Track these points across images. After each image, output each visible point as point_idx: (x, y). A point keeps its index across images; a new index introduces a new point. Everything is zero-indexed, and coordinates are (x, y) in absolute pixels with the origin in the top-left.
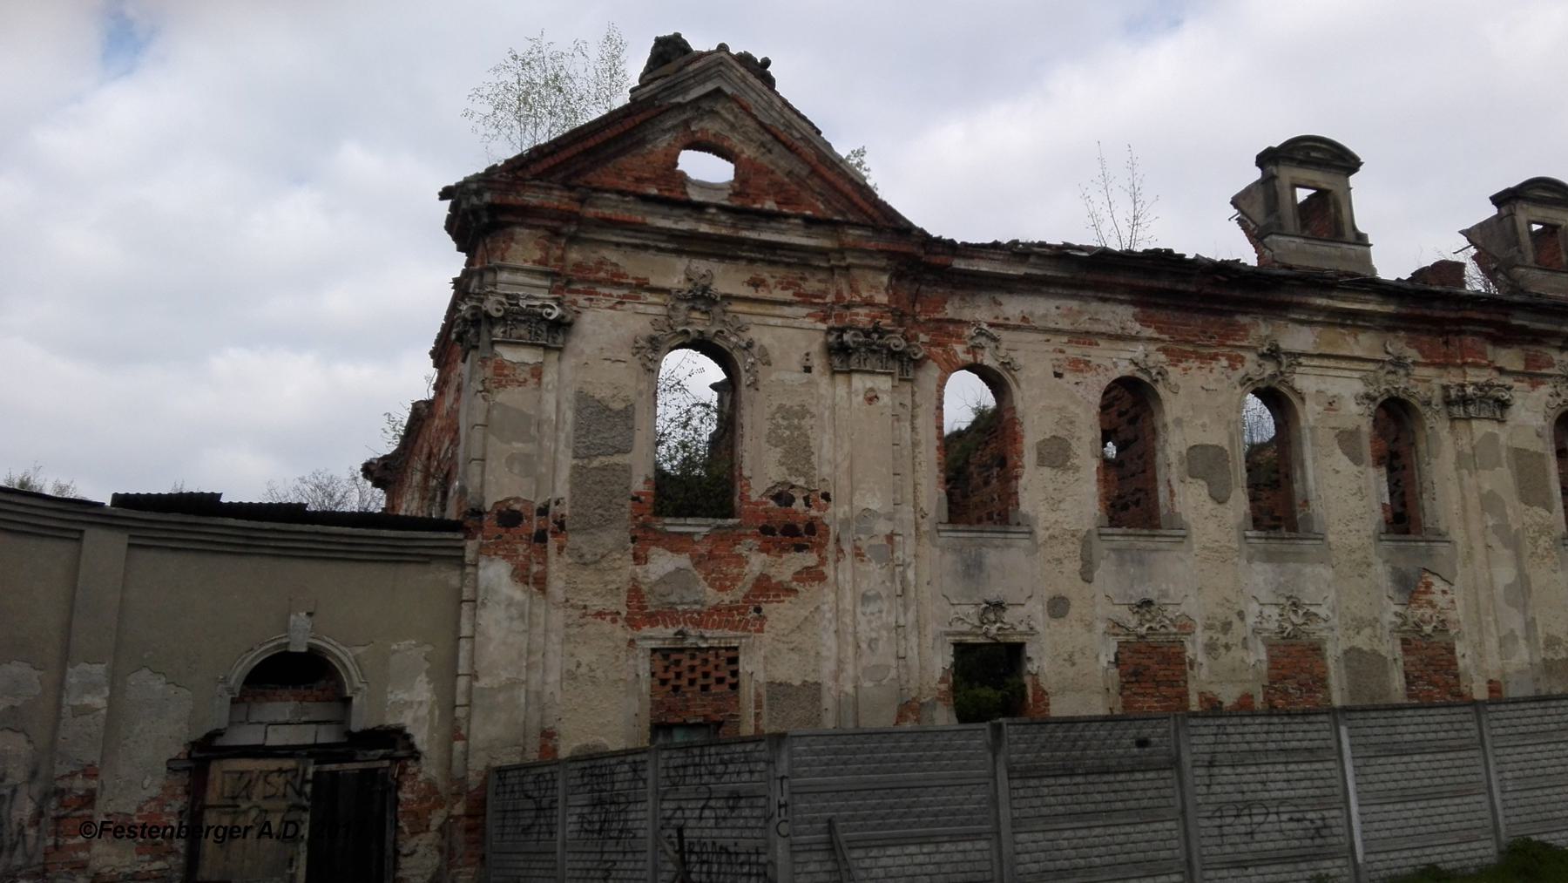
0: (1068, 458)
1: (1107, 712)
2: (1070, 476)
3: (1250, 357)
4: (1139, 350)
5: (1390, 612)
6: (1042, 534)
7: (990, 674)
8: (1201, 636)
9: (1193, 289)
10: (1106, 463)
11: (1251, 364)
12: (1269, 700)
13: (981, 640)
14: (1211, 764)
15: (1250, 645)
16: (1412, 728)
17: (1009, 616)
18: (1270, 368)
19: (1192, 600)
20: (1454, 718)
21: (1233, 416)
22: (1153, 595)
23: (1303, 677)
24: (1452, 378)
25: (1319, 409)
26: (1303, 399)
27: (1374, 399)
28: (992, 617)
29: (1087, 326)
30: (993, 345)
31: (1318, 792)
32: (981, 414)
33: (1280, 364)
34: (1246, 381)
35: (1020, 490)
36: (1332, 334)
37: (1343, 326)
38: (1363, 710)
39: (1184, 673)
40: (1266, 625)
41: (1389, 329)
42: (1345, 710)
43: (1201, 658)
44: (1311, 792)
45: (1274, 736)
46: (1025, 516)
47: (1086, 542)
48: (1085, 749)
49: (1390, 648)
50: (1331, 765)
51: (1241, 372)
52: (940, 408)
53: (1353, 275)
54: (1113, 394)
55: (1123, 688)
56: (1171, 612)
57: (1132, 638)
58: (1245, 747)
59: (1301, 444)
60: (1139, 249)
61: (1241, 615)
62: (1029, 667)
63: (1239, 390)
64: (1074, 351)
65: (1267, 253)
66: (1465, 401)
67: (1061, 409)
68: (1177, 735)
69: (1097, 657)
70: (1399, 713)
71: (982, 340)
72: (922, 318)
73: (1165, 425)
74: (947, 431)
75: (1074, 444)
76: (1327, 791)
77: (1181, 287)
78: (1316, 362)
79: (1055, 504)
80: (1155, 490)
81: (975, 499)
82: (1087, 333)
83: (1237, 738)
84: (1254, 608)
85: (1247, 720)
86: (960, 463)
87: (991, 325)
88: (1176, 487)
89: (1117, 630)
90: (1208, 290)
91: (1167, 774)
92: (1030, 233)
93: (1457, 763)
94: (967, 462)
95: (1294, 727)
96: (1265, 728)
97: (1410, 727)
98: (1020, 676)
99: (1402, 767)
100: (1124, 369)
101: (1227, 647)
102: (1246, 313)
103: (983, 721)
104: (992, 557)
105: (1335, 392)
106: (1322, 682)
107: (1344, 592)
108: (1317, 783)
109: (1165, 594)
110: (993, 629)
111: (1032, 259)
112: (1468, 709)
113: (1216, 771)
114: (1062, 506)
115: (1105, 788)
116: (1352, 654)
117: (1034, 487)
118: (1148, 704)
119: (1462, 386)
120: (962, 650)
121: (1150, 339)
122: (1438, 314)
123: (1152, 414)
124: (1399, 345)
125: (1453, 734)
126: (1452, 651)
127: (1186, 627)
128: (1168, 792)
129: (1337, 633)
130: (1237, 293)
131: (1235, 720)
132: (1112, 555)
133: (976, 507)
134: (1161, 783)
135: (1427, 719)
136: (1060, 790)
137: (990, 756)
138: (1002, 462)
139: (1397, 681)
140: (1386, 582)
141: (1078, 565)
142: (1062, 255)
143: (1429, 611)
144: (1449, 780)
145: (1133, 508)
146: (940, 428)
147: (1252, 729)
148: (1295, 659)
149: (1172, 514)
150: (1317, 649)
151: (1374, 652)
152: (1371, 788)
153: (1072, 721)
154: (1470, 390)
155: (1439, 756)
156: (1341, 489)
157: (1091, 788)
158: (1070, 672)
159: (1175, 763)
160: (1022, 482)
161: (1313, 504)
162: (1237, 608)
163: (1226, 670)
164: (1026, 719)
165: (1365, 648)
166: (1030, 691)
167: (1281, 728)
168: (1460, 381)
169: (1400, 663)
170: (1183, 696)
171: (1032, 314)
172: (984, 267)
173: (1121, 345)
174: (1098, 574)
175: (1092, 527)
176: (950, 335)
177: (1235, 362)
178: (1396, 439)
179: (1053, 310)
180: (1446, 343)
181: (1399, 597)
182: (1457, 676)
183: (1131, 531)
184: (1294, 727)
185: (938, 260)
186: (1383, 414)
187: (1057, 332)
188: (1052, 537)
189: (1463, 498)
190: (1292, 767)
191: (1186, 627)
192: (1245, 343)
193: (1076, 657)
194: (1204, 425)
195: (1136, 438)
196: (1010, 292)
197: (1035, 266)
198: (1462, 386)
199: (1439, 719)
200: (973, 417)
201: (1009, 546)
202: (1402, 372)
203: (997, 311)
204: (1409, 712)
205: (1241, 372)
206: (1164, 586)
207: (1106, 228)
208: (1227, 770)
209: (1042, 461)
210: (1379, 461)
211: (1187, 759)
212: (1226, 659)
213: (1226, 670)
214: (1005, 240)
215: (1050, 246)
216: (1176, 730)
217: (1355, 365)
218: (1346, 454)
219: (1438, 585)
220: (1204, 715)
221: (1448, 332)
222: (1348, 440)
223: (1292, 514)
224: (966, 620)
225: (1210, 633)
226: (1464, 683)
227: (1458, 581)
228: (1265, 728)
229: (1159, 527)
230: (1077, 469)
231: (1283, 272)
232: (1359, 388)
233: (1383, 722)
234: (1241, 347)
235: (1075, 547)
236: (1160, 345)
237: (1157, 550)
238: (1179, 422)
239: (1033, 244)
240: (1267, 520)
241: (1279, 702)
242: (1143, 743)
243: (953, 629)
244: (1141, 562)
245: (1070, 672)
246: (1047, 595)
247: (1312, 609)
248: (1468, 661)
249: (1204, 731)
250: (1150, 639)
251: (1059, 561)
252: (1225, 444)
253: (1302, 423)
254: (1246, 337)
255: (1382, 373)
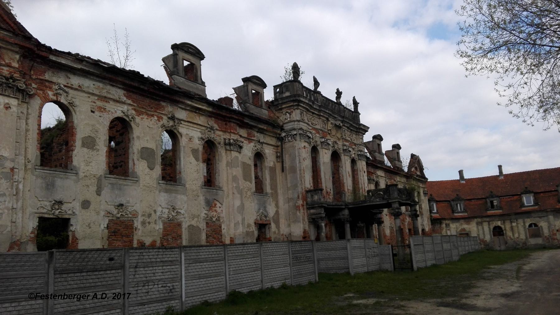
0: (95, 145)
1: (101, 247)
2: (95, 153)
3: (165, 118)
4: (125, 108)
6: (81, 175)
7: (54, 231)
8: (140, 219)
9: (146, 88)
10: (111, 150)
11: (165, 120)
12: (162, 243)
13: (51, 216)
14: (136, 267)
15: (157, 222)
16: (205, 253)
17: (64, 207)
18: (171, 123)
19: (138, 205)
20: (217, 250)
21: (158, 138)
22: (124, 202)
23: (174, 235)
24: (227, 136)
25: (187, 140)
26: (181, 136)
27: (204, 140)
28: (57, 207)
29: (105, 95)
30: (65, 94)
31: (172, 276)
32: (60, 122)
33: (175, 122)
34: (163, 126)
35: (73, 156)
36: (192, 115)
37: (196, 112)
38: (190, 247)
39: (133, 232)
40: (163, 216)
41: (210, 117)
42: (185, 247)
43: (140, 227)
44: (170, 276)
45: (160, 256)
46: (75, 167)
47: (99, 179)
48: (88, 262)
49: (203, 225)
50: (177, 266)
51: (161, 123)
52: (40, 117)
53: (199, 95)
54: (115, 123)
55: (109, 238)
56: (130, 209)
57: (114, 218)
58: (149, 260)
59: (180, 152)
60: (127, 69)
61: (155, 211)
62: (71, 228)
63: (160, 129)
64: (99, 103)
65: (173, 81)
66: (230, 144)
67: (93, 125)
68: (125, 255)
69: (100, 225)
70: (201, 248)
71: (61, 92)
72: (34, 77)
73: (133, 138)
74: (43, 127)
75: (97, 140)
76: (175, 276)
77: (142, 87)
78: (186, 124)
79: (88, 163)
80: (128, 162)
81: (55, 157)
82: (105, 97)
83: (147, 257)
84: (160, 209)
85: (151, 250)
86: (49, 141)
87: (65, 86)
88: (136, 162)
89: (108, 215)
90: (152, 90)
91: (119, 271)
92: (85, 52)
93: (217, 265)
94: (52, 141)
95: (167, 253)
96: (157, 253)
97: (204, 253)
98: (67, 232)
99: (200, 267)
100: (119, 114)
101: (149, 223)
102: (164, 102)
103: (46, 251)
104: (59, 182)
105: (192, 135)
106: (180, 237)
107: (189, 206)
108: (172, 273)
109: (128, 202)
110: (57, 212)
111: (84, 63)
112: (222, 247)
113: (137, 269)
114: (91, 164)
115: (94, 277)
116: (191, 227)
117: (79, 155)
118: (118, 244)
119: (230, 139)
120: (42, 220)
121: (130, 104)
122: (224, 114)
123: (129, 133)
124: (212, 122)
125: (216, 256)
126: (221, 227)
127: (135, 215)
128: (119, 278)
129: (186, 219)
130: (161, 94)
131: (147, 250)
132: (110, 186)
133: (55, 161)
134: (117, 275)
135: (210, 250)
136: (76, 278)
137: (47, 265)
138: (67, 143)
139: (204, 237)
141: (95, 188)
142: (97, 64)
143: (215, 213)
144: (214, 271)
145: (119, 168)
146: (39, 125)
147: (153, 253)
148: (172, 228)
149: (134, 172)
150: (179, 225)
151: (198, 227)
152: (189, 274)
153: (84, 251)
154: (232, 141)
155: (212, 263)
156: (191, 169)
157: (89, 277)
158: (88, 231)
159: (123, 267)
160: (75, 153)
161: (183, 174)
162: (154, 209)
163: (147, 232)
164: (65, 250)
165: (195, 225)
166: (70, 238)
167: (162, 253)
168: (229, 137)
169: (205, 231)
170: (131, 241)
171: (83, 85)
172: (63, 61)
173: (118, 104)
174: (103, 193)
175: (102, 174)
176: (46, 87)
177: (160, 119)
178: (210, 154)
179: (92, 85)
180: (226, 124)
181: (207, 208)
182: (221, 236)
183: (117, 177)
184: (167, 253)
185: (44, 54)
186: (206, 145)
187: (93, 94)
188: (86, 176)
189: (228, 176)
190: (164, 267)
191: (135, 215)
192: (163, 112)
193: (92, 225)
194: (147, 140)
195: (122, 142)
196: (74, 74)
197: (85, 66)
198: (230, 139)
199: (213, 250)
200: (56, 123)
201: (67, 178)
202: (212, 132)
203: (68, 81)
204: (204, 248)
205: (161, 123)
206: (128, 199)
207: (116, 57)
208: (142, 269)
209: (84, 145)
210: (204, 162)
211: (127, 265)
212: (148, 227)
213: (147, 232)
214: (73, 52)
215: (92, 59)
216: (125, 255)
217: (199, 127)
218: (194, 158)
219: (218, 205)
220: (136, 249)
221: (226, 121)
222: (194, 152)
223: (176, 176)
224: (45, 207)
225: (144, 217)
226: (223, 238)
227: (224, 204)
228: (157, 253)
229: (128, 176)
230: (98, 150)
231: (178, 89)
232: (200, 135)
233: (196, 251)
234: (162, 114)
235: (95, 181)
236: (133, 107)
237: (127, 185)
238: (138, 137)
239: (85, 57)
240: (168, 178)
241: (165, 244)
242: (111, 259)
243: (39, 211)
244: (120, 189)
245: (88, 231)
246: (82, 199)
247: (179, 211)
248: (225, 230)
249: (135, 254)
250: (121, 219)
251: (88, 186)
252: (154, 148)
253: (181, 144)
254: (164, 110)
255: (207, 131)
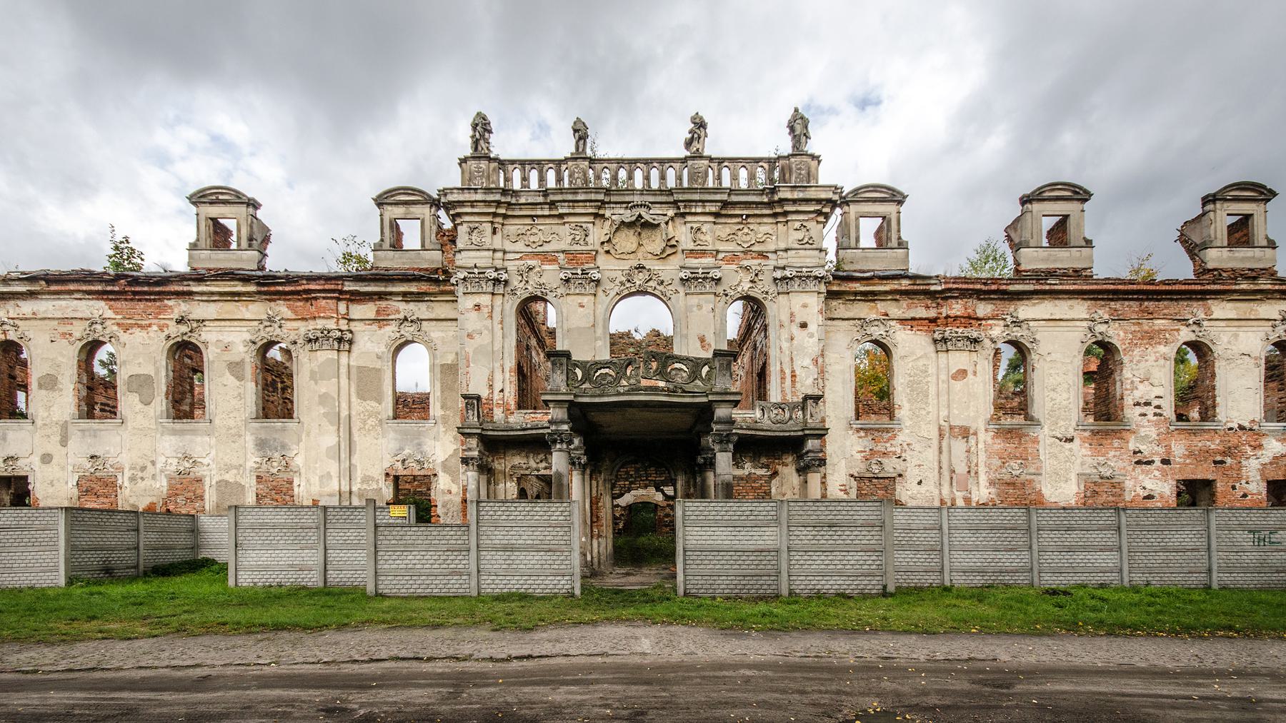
5: (252, 460)
61: (153, 463)
84: (163, 459)
106: (202, 498)
116: (223, 485)
140: (250, 445)
150: (199, 481)
212: (141, 484)
232: (248, 337)
